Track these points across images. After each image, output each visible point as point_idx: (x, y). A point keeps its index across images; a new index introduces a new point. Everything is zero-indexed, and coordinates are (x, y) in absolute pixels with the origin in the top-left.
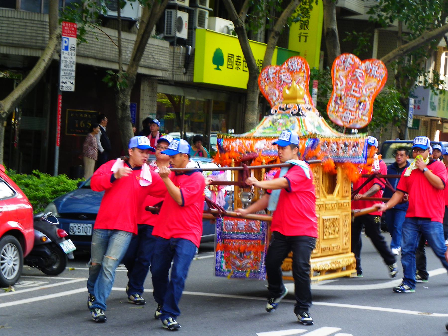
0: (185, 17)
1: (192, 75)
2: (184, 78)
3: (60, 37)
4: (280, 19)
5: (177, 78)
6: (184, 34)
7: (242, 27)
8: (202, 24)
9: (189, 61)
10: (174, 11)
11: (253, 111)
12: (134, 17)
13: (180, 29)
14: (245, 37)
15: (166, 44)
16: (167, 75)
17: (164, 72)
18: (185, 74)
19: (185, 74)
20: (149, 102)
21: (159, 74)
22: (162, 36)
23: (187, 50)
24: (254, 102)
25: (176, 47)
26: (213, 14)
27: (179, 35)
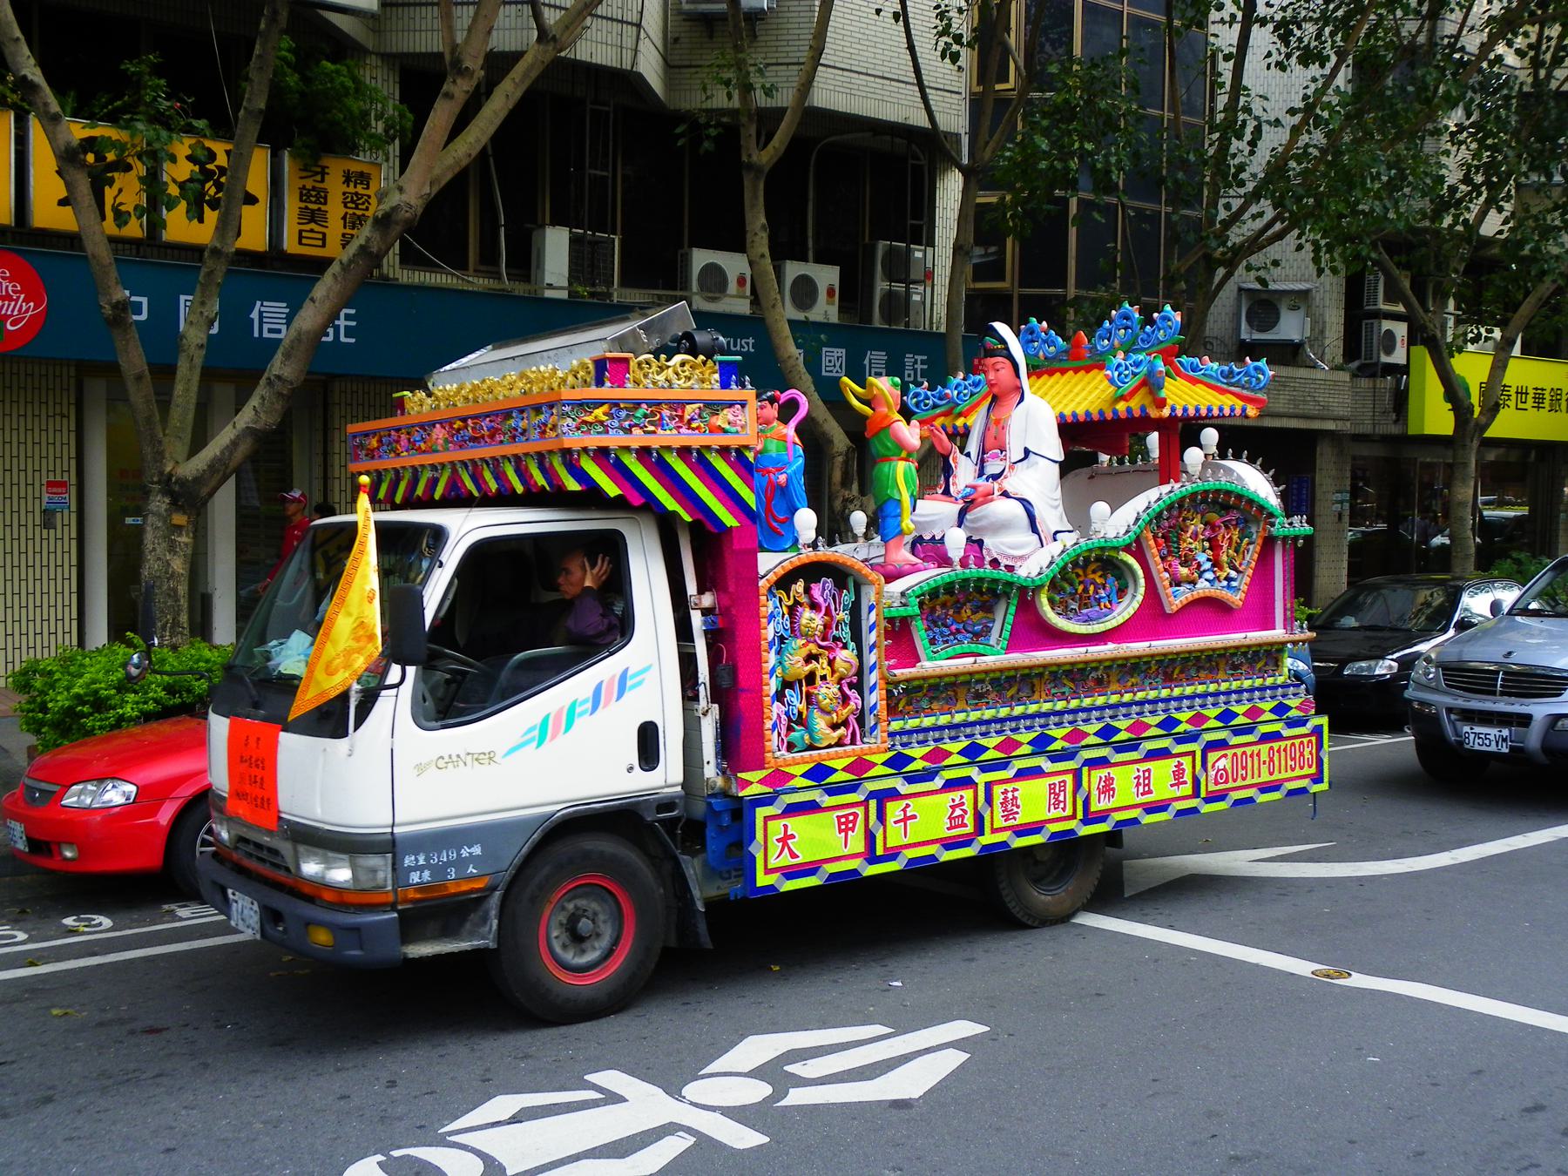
0: (1401, 330)
1: (1406, 424)
2: (1394, 430)
4: (1517, 316)
5: (1381, 430)
6: (1398, 356)
7: (1434, 337)
9: (1400, 401)
10: (1376, 322)
11: (1464, 481)
12: (1296, 337)
13: (1390, 350)
14: (1440, 353)
15: (1345, 376)
16: (1346, 427)
17: (1340, 423)
18: (1396, 422)
19: (1396, 422)
20: (1334, 472)
21: (1330, 426)
22: (1356, 364)
23: (1399, 382)
24: (1466, 465)
25: (1378, 381)
27: (1385, 359)
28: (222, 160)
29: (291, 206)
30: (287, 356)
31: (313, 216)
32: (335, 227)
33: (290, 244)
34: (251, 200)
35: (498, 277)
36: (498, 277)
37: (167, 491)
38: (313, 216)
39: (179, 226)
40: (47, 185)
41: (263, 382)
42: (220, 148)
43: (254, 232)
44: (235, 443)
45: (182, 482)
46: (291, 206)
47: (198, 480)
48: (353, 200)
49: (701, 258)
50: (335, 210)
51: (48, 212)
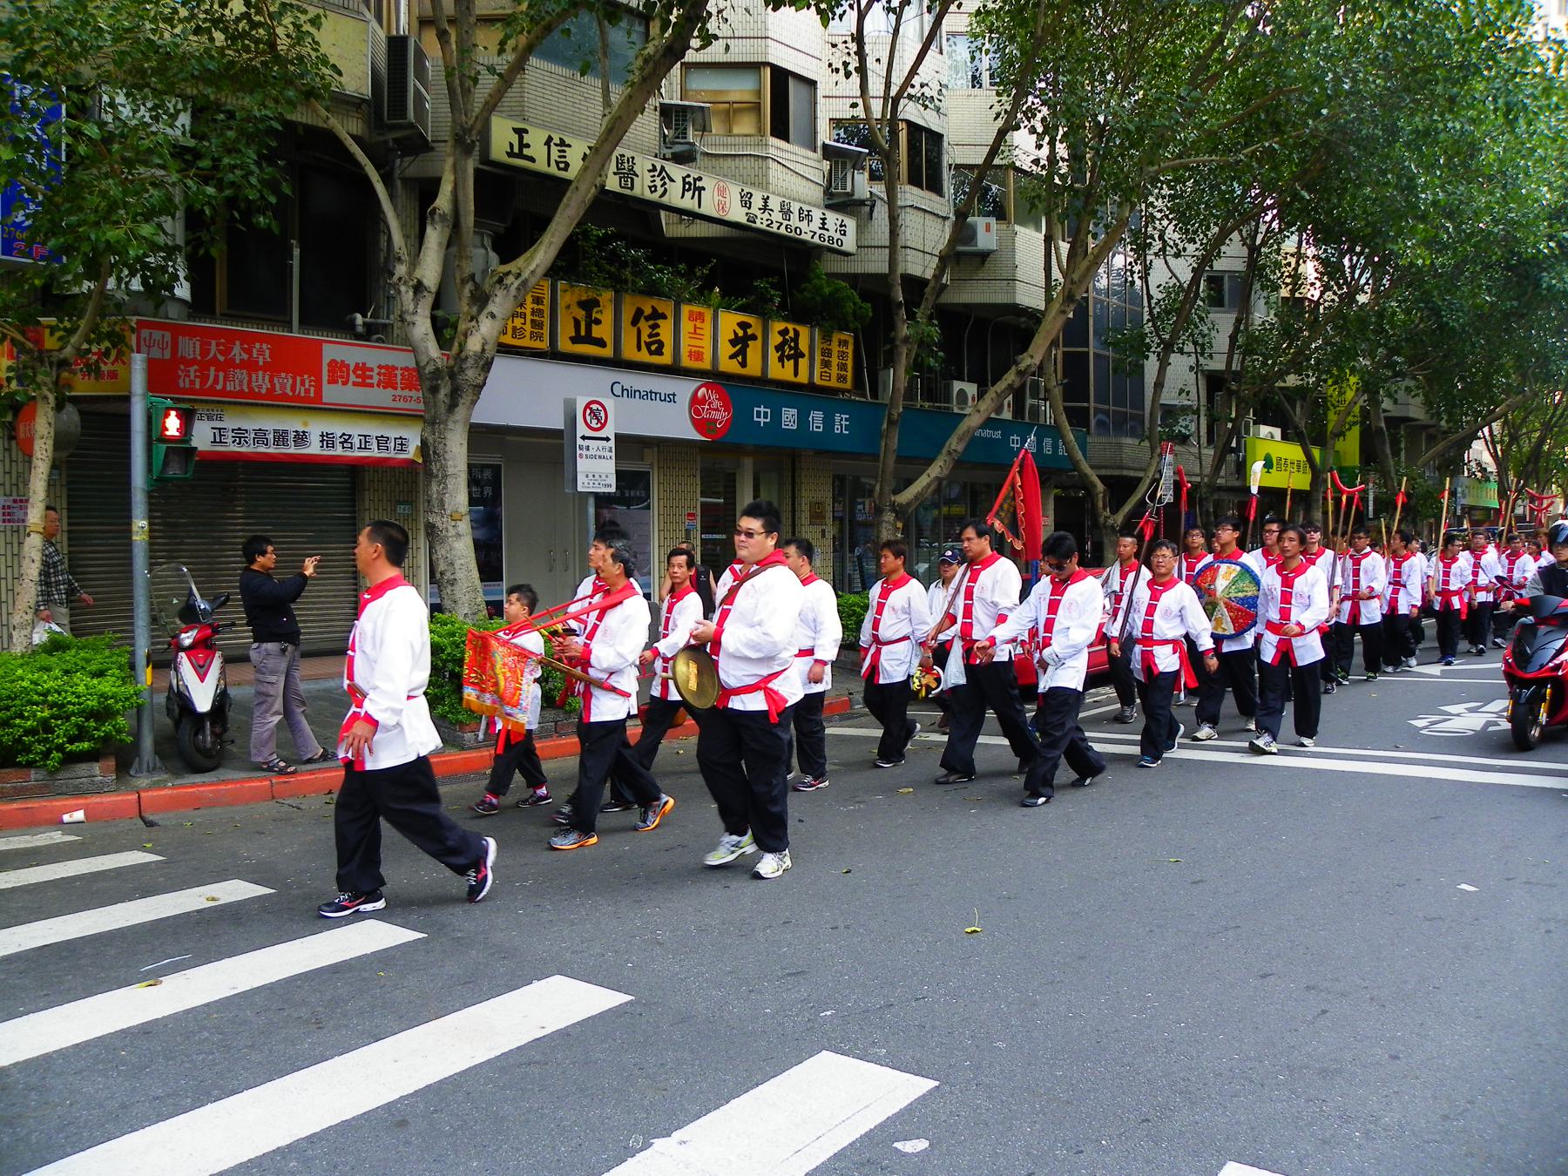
2: (1237, 484)
3: (1160, 455)
8: (1247, 432)
26: (1255, 423)
28: (791, 334)
29: (818, 358)
30: (960, 439)
31: (826, 364)
32: (834, 371)
33: (817, 380)
34: (803, 356)
35: (864, 396)
36: (864, 396)
37: (893, 510)
38: (826, 364)
39: (780, 371)
40: (726, 350)
41: (944, 451)
42: (790, 327)
43: (803, 378)
44: (929, 485)
45: (900, 505)
46: (818, 358)
47: (909, 504)
48: (842, 355)
49: (957, 386)
50: (835, 361)
51: (729, 366)
